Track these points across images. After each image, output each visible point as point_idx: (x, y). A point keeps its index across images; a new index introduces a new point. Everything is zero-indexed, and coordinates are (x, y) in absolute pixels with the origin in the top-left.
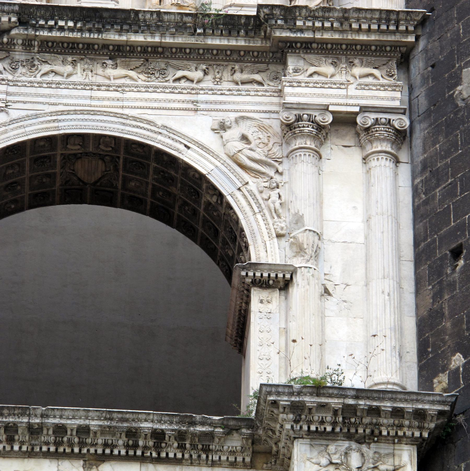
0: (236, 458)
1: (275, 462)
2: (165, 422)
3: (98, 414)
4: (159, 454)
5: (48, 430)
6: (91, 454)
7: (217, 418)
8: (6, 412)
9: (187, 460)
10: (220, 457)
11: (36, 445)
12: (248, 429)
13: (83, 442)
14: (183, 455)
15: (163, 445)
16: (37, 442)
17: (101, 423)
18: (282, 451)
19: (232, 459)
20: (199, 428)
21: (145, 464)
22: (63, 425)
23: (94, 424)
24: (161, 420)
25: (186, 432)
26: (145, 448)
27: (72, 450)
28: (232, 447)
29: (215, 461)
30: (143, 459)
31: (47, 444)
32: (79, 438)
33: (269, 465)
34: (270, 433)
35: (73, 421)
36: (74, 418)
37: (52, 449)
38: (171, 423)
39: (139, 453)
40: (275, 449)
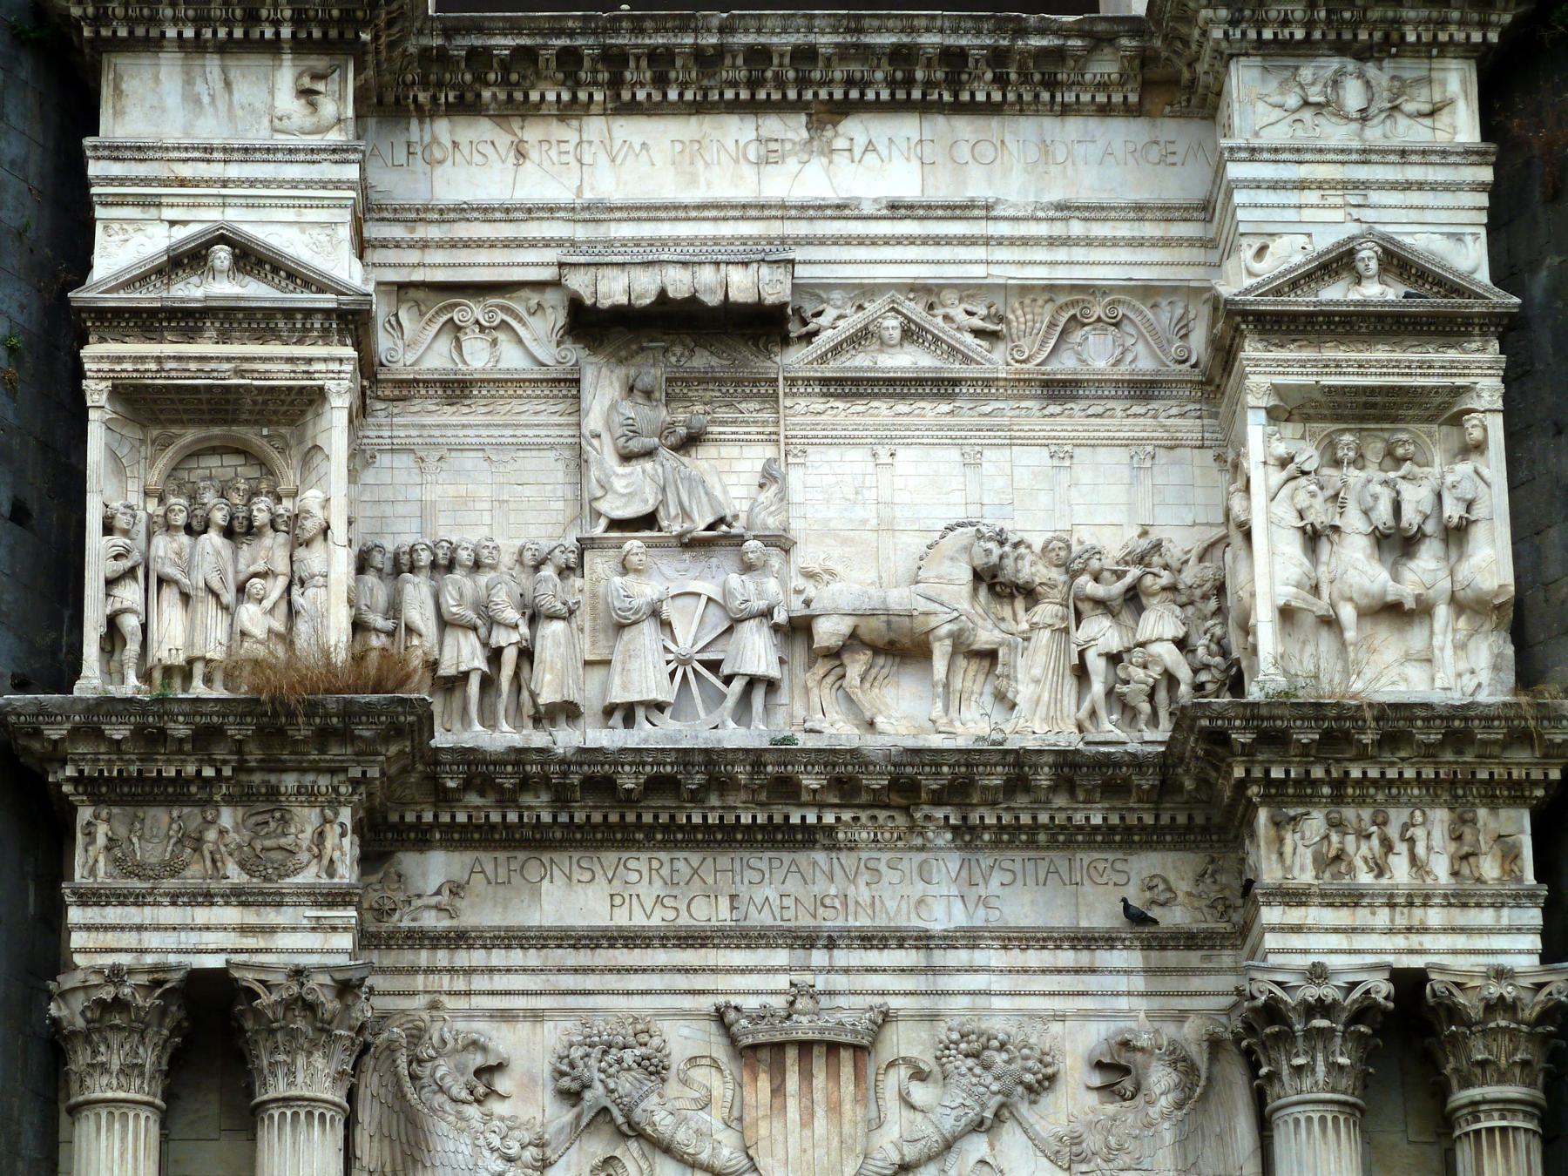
0: (1109, 97)
1: (1189, 100)
2: (967, 32)
3: (832, 21)
4: (956, 96)
5: (734, 57)
6: (822, 102)
7: (1071, 18)
8: (649, 24)
9: (1012, 104)
10: (1078, 97)
11: (711, 88)
12: (1132, 37)
13: (804, 79)
14: (1004, 96)
15: (964, 77)
16: (713, 83)
17: (839, 39)
18: (1202, 78)
19: (1101, 98)
20: (1036, 42)
21: (929, 116)
22: (763, 45)
23: (825, 40)
24: (959, 28)
25: (1008, 50)
26: (929, 84)
27: (784, 95)
28: (1102, 75)
29: (1069, 105)
30: (925, 108)
31: (734, 84)
32: (797, 71)
33: (1177, 107)
34: (1179, 45)
35: (785, 39)
36: (785, 31)
37: (744, 95)
38: (979, 32)
39: (916, 94)
40: (1186, 75)
